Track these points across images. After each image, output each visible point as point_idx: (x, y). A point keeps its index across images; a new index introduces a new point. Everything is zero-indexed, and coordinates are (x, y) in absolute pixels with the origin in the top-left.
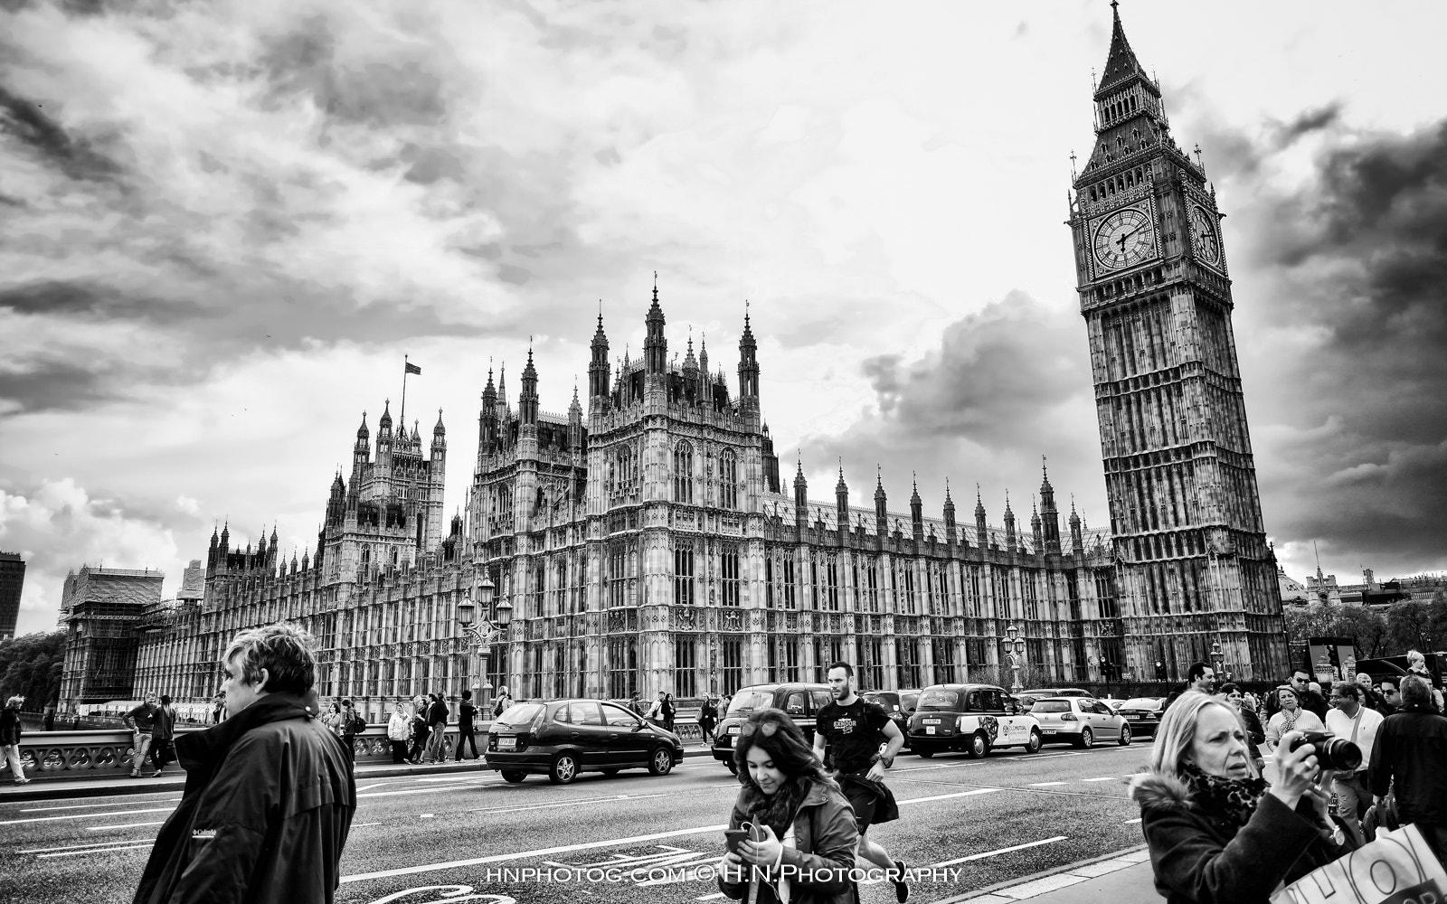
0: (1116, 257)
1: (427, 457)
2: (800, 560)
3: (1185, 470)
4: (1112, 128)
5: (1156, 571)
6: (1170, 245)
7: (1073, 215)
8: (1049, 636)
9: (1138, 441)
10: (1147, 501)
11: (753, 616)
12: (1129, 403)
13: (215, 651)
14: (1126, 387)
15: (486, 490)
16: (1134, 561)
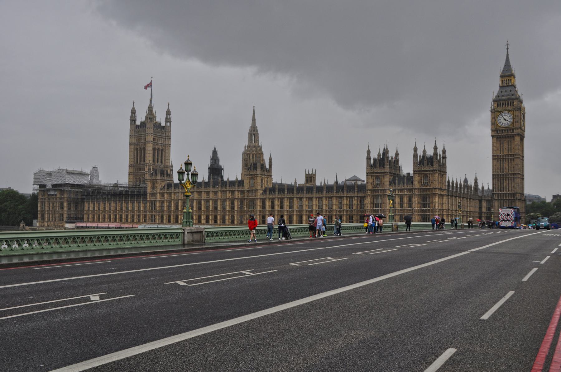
0: (503, 123)
1: (163, 124)
2: (449, 199)
3: (512, 179)
4: (504, 87)
5: (502, 201)
6: (517, 124)
7: (492, 109)
8: (475, 215)
9: (502, 170)
10: (502, 185)
11: (445, 211)
12: (500, 161)
13: (162, 207)
14: (500, 157)
15: (370, 177)
16: (497, 199)
